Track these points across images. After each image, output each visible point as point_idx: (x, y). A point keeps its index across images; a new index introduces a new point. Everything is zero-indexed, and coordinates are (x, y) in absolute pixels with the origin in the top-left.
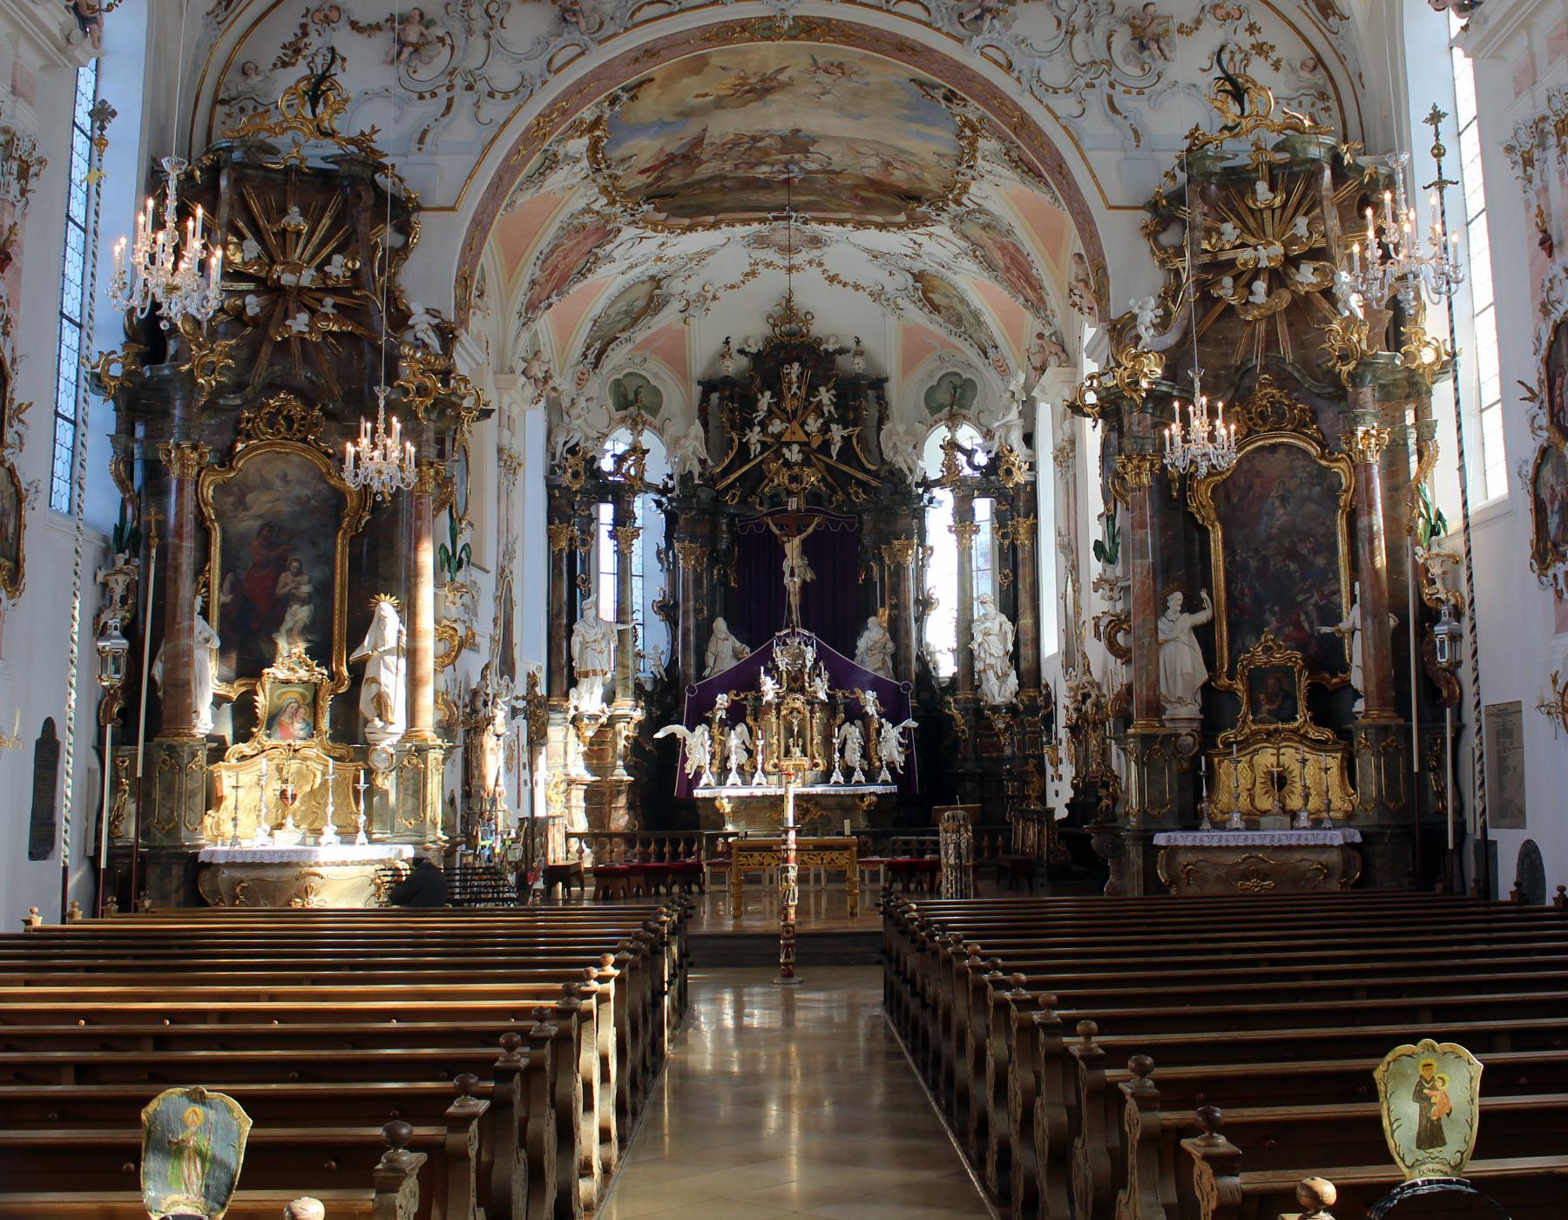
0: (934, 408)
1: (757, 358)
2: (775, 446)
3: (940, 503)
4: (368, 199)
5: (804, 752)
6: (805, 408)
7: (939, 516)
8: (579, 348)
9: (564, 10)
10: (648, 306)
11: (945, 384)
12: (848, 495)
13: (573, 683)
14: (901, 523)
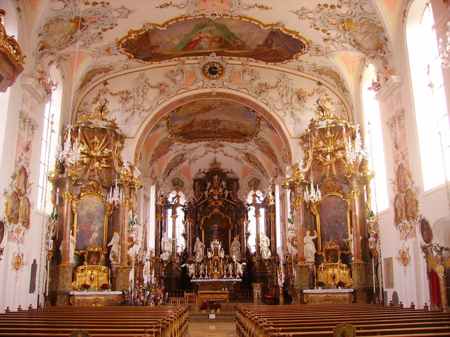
0: (250, 186)
1: (207, 174)
4: (114, 135)
5: (218, 271)
7: (251, 213)
9: (161, 91)
10: (181, 161)
11: (253, 180)
13: (161, 253)
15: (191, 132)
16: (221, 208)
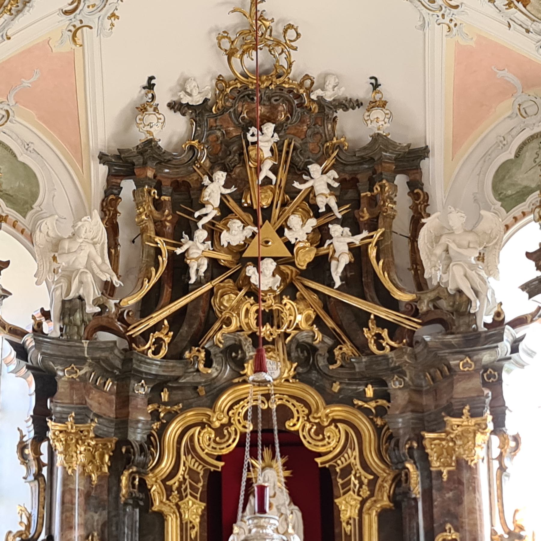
1: (198, 113)
2: (233, 268)
3: (531, 354)
6: (284, 204)
11: (528, 156)
12: (362, 348)
14: (462, 389)
16: (304, 356)
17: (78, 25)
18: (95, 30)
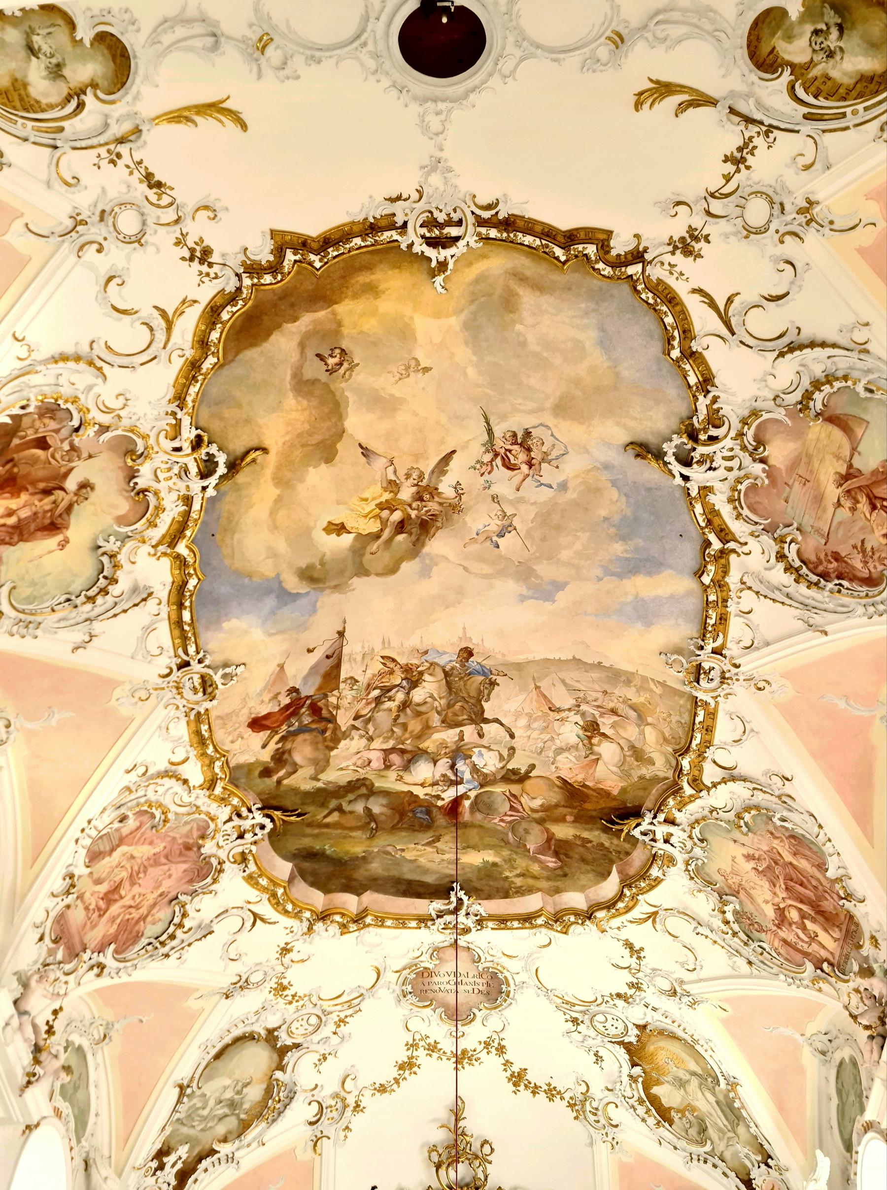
8: (150, 1143)
15: (324, 796)
17: (319, 1135)
18: (332, 1140)
